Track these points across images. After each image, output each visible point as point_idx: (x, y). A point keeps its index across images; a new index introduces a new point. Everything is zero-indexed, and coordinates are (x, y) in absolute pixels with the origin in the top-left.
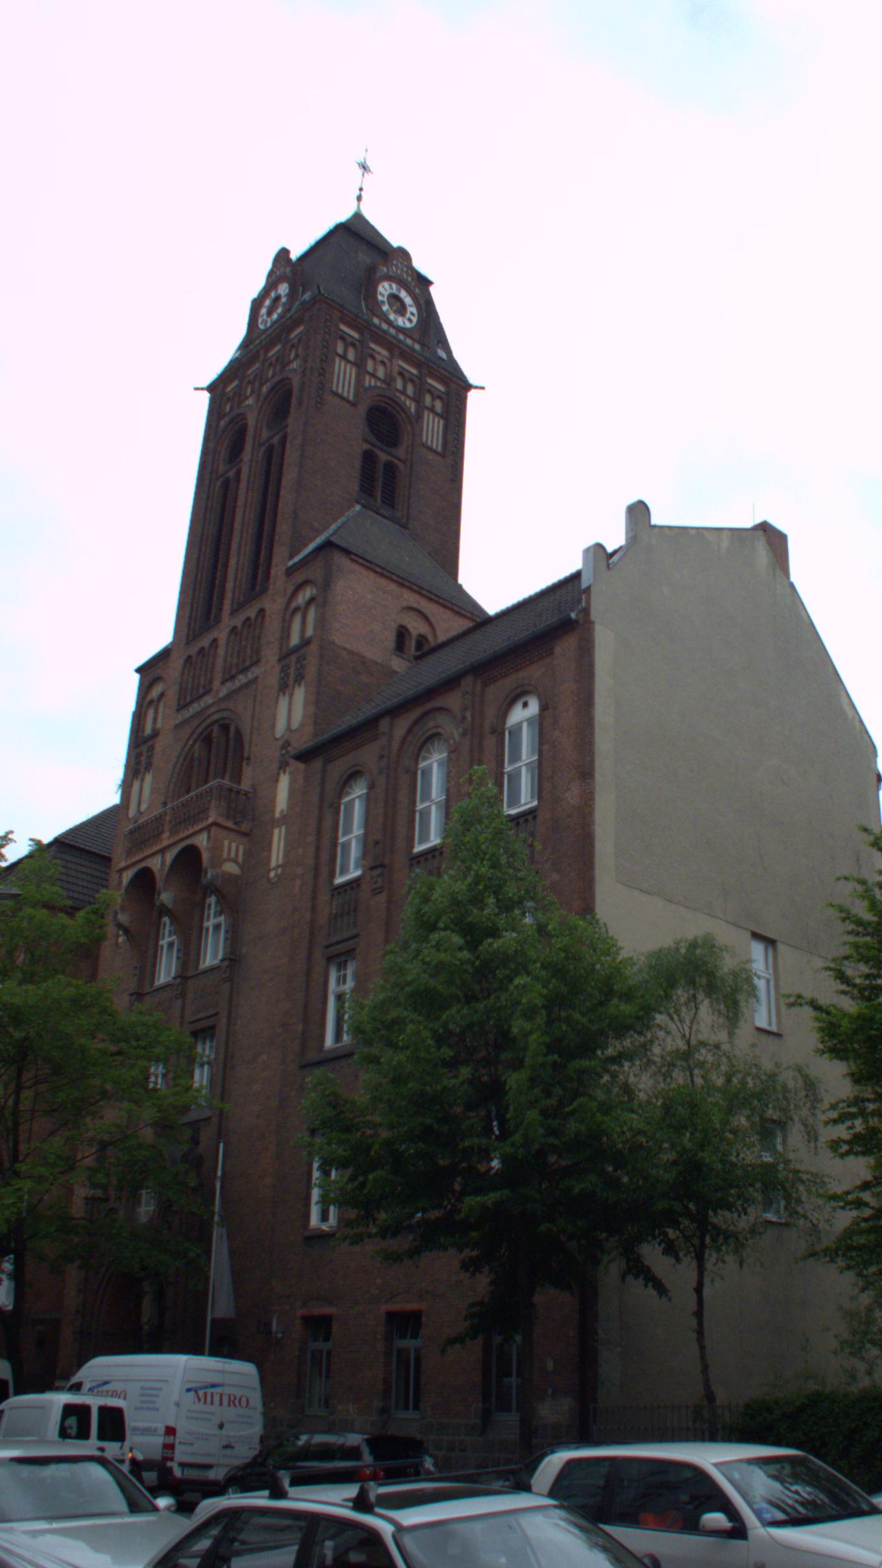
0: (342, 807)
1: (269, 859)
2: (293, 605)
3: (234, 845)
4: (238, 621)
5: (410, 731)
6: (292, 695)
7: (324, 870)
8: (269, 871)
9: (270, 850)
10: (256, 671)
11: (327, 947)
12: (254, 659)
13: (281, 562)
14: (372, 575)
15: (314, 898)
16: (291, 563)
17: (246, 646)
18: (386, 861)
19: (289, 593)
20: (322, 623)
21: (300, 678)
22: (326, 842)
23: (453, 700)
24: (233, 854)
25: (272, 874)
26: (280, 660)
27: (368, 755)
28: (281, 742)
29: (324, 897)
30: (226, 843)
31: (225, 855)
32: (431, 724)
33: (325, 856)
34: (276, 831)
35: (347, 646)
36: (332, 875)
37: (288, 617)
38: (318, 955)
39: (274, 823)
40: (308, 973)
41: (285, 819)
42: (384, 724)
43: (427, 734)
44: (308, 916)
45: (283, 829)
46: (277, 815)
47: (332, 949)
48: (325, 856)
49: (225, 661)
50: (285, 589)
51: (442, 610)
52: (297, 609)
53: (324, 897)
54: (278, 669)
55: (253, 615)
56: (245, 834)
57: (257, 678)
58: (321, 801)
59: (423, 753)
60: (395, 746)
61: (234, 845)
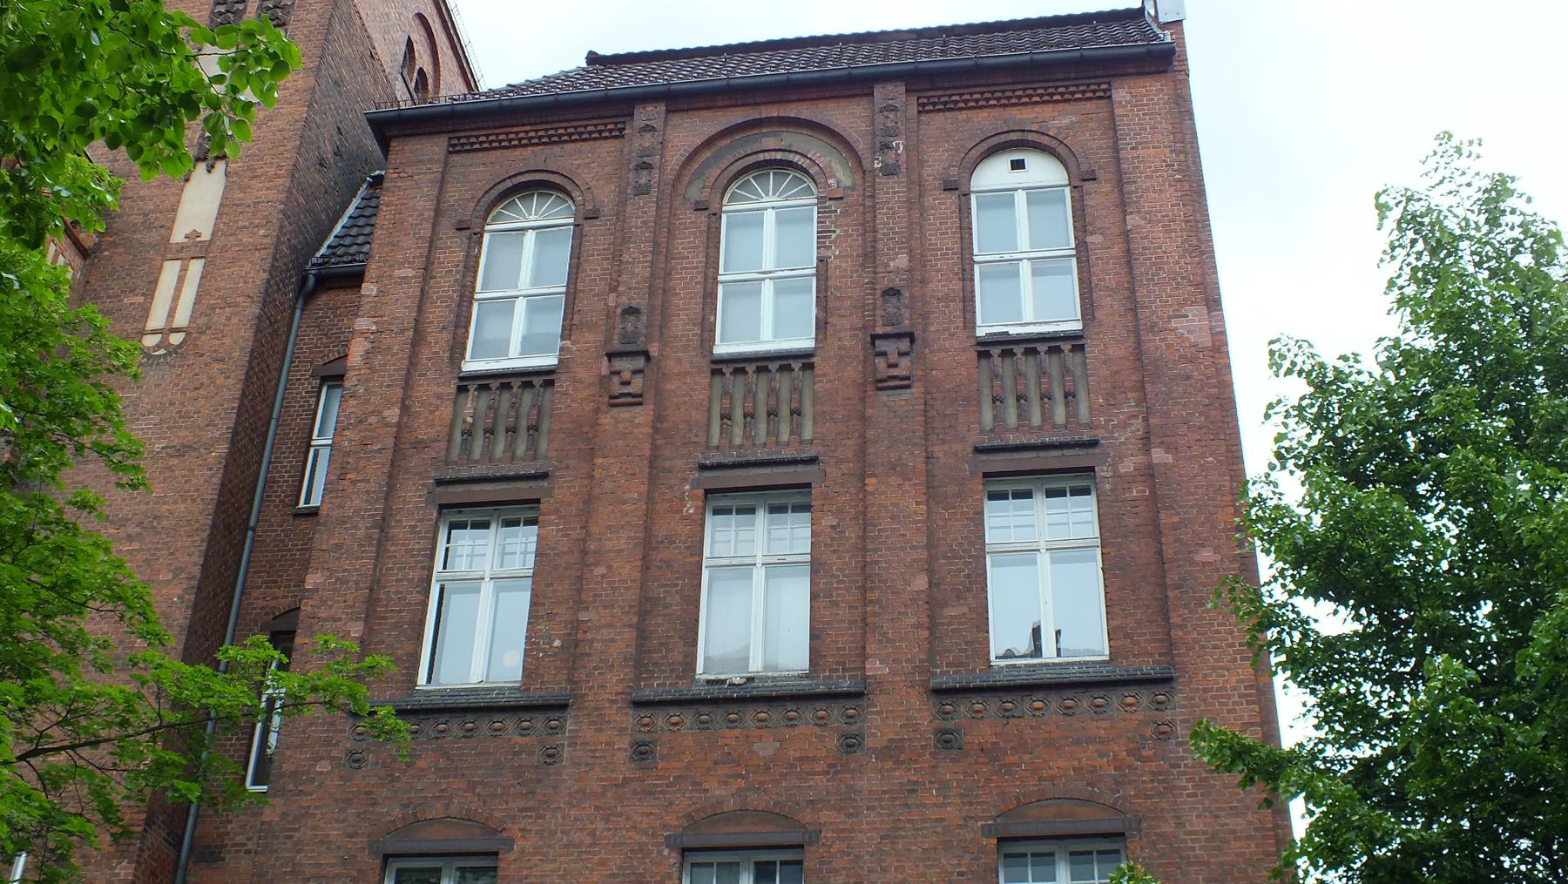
0: (486, 237)
1: (146, 310)
5: (709, 143)
7: (437, 342)
8: (142, 333)
9: (150, 295)
11: (440, 483)
15: (407, 385)
18: (654, 350)
22: (444, 285)
23: (846, 116)
25: (150, 341)
27: (590, 162)
29: (433, 388)
32: (769, 143)
33: (438, 313)
34: (170, 270)
36: (457, 350)
38: (414, 495)
39: (167, 251)
40: (383, 525)
41: (195, 248)
42: (648, 114)
43: (761, 157)
44: (393, 414)
45: (196, 267)
46: (178, 237)
47: (451, 489)
48: (438, 313)
51: (450, 52)
53: (433, 388)
56: (84, 252)
58: (438, 212)
59: (733, 188)
60: (675, 158)
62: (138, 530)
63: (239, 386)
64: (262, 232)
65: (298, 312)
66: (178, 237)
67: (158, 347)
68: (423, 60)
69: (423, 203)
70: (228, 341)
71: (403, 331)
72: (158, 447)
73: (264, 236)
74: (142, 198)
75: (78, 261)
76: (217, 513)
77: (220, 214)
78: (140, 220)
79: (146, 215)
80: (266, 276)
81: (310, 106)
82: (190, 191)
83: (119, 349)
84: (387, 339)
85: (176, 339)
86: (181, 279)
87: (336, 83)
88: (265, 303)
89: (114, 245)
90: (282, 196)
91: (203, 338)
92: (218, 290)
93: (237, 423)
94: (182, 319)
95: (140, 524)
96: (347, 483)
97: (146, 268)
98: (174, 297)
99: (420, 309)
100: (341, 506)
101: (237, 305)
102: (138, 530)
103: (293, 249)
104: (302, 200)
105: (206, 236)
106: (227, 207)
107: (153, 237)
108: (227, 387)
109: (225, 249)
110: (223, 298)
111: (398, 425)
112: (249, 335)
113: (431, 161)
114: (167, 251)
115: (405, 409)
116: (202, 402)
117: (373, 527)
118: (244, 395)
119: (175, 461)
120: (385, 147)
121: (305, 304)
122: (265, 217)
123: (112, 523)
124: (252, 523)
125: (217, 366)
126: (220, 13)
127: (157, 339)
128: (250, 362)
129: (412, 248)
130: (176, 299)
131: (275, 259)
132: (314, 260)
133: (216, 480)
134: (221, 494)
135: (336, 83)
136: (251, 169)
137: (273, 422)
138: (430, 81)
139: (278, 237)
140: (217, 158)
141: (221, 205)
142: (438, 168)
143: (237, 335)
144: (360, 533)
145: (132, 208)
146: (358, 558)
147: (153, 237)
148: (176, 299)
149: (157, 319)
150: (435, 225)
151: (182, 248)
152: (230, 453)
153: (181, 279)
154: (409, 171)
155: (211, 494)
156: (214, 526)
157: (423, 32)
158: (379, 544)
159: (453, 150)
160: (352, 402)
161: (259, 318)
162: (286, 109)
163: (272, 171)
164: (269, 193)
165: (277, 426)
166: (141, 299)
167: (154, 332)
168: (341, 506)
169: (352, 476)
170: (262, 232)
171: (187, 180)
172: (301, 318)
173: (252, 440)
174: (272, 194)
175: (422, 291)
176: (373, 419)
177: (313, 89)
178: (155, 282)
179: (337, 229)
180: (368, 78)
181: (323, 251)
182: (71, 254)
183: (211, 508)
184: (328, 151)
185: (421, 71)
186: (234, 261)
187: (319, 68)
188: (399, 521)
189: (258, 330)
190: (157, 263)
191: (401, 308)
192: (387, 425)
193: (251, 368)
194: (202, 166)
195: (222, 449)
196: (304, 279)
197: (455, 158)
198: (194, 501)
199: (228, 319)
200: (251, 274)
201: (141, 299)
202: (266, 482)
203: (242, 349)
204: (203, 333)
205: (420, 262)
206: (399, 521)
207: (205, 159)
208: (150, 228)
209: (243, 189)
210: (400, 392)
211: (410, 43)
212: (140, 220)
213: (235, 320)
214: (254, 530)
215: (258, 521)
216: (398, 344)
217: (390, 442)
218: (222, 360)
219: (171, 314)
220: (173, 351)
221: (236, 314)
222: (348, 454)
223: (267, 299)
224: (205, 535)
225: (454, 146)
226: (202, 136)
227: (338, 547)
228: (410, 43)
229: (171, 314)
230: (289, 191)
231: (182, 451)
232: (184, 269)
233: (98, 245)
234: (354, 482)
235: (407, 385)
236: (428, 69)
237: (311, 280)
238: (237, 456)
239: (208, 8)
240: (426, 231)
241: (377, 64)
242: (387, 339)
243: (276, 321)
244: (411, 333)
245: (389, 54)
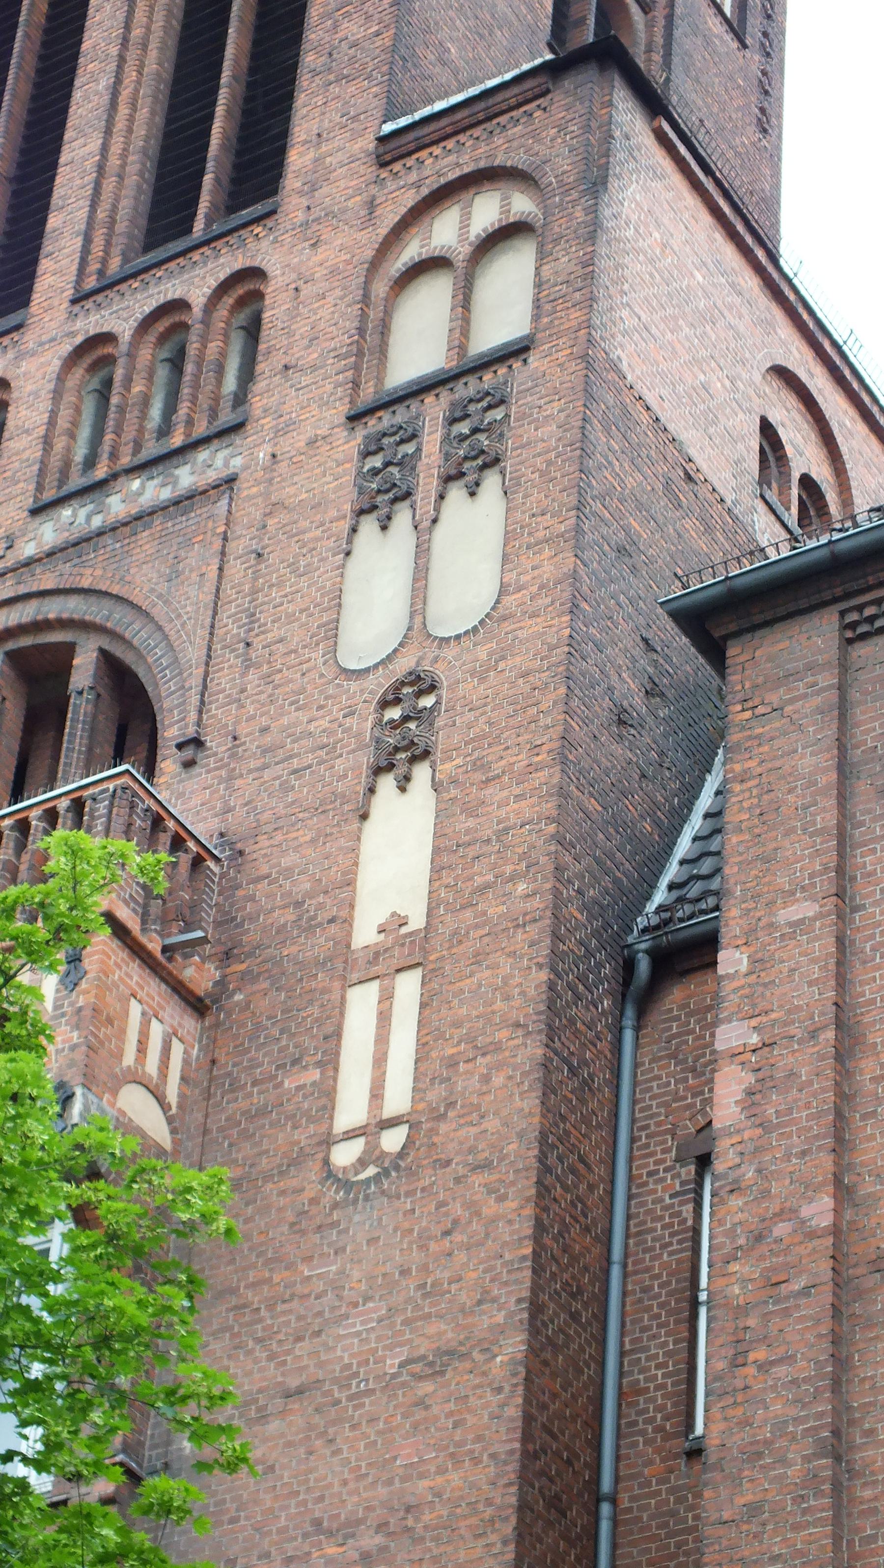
1: (327, 1095)
2: (412, 251)
3: (157, 1030)
4: (121, 315)
6: (425, 530)
8: (328, 1141)
9: (330, 1062)
10: (215, 462)
12: (226, 417)
13: (330, 131)
14: (706, 218)
15: (841, 1141)
16: (388, 128)
17: (145, 401)
19: (390, 217)
20: (574, 296)
21: (469, 467)
24: (152, 1066)
25: (344, 1155)
26: (354, 418)
28: (379, 684)
30: (135, 1010)
31: (129, 1058)
35: (651, 399)
37: (380, 289)
39: (348, 966)
44: (820, 1210)
45: (408, 987)
46: (365, 934)
49: (47, 442)
50: (371, 205)
52: (434, 264)
54: (349, 444)
55: (198, 297)
56: (197, 1005)
57: (231, 480)
58: (845, 770)
61: (157, 1030)
62: (379, 1540)
63: (529, 1211)
64: (522, 887)
65: (628, 1036)
66: (365, 934)
67: (362, 1163)
68: (805, 455)
69: (813, 761)
70: (492, 1124)
71: (813, 1034)
72: (392, 1364)
73: (529, 895)
74: (288, 872)
75: (189, 1024)
76: (524, 1479)
77: (437, 870)
78: (290, 915)
79: (298, 904)
80: (544, 975)
81: (574, 609)
82: (374, 834)
83: (189, 1190)
84: (783, 1059)
85: (393, 1140)
86: (384, 1018)
87: (621, 550)
88: (552, 1033)
89: (248, 977)
90: (549, 807)
91: (443, 1127)
92: (457, 1024)
93: (535, 1289)
94: (398, 1098)
95: (382, 1527)
96: (751, 1370)
97: (315, 1010)
98: (376, 1058)
99: (842, 981)
100: (746, 1422)
101: (497, 1047)
102: (379, 1540)
103: (591, 908)
104: (593, 805)
105: (417, 921)
106: (447, 854)
107: (319, 944)
108: (503, 1221)
109: (457, 938)
110: (470, 1039)
111: (836, 1230)
112: (531, 1103)
113: (810, 668)
114: (348, 966)
115: (843, 1191)
116: (461, 1257)
117: (817, 1456)
118: (540, 1227)
119: (427, 1387)
120: (715, 653)
121: (641, 1014)
122: (523, 856)
123: (330, 1534)
124: (606, 1484)
125: (477, 1180)
126: (375, 472)
127: (357, 1147)
128: (542, 1159)
129: (805, 856)
130: (380, 1060)
131: (556, 937)
132: (641, 922)
133: (514, 1411)
134: (527, 1437)
135: (621, 550)
136: (479, 765)
137: (616, 1272)
138: (831, 497)
139: (556, 893)
140: (413, 760)
141: (437, 851)
142: (828, 679)
143: (508, 1109)
144: (794, 1472)
145: (270, 896)
146: (796, 1527)
147: (319, 944)
148: (380, 1060)
149: (351, 1109)
150: (843, 799)
151: (376, 954)
152: (533, 1351)
153: (384, 1018)
154: (774, 698)
155: (505, 1441)
156: (523, 1507)
157: (792, 401)
158: (837, 1487)
159: (853, 635)
160: (736, 1202)
161: (545, 1065)
162: (535, 626)
163: (521, 760)
164: (522, 806)
165: (625, 1275)
166: (315, 1075)
167: (350, 1135)
168: (746, 1422)
169: (760, 1354)
170: (522, 887)
171: (364, 817)
172: (637, 1046)
173: (575, 1316)
174: (527, 808)
175: (841, 942)
176: (781, 1229)
177: (574, 575)
178: (338, 1034)
179: (684, 846)
180: (690, 525)
181: (660, 896)
182: (175, 1013)
183: (513, 1468)
184: (630, 690)
185: (806, 482)
186: (478, 958)
187: (578, 530)
188: (871, 1432)
189: (548, 1089)
190: (336, 996)
191: (806, 989)
192: (812, 1235)
193: (545, 1168)
194: (387, 784)
195: (514, 1345)
196: (629, 966)
197: (862, 651)
198: (476, 1461)
199: (486, 1079)
200: (515, 979)
201: (315, 1075)
202: (621, 1395)
203: (520, 1135)
204: (442, 1117)
205: (825, 884)
206: (871, 1432)
207: (391, 767)
208: (310, 929)
209: (470, 811)
210: (827, 1161)
211: (767, 429)
212: (290, 915)
213: (498, 1080)
214: (614, 1501)
215: (617, 1479)
216: (807, 1062)
217: (824, 1268)
218: (485, 1166)
219: (377, 1094)
220: (392, 1166)
221: (499, 1066)
222: (742, 1311)
223: (556, 1021)
224: (508, 1528)
225: (853, 626)
226: (379, 723)
227: (754, 1509)
228: (767, 429)
229: (377, 1094)
230: (562, 793)
231: (437, 1364)
232: (387, 997)
233: (221, 984)
234: (764, 1367)
235: (841, 1141)
236: (822, 474)
237: (643, 966)
238: (547, 1355)
239: (351, 468)
240: (826, 816)
241: (703, 491)
242: (783, 1059)
243: (585, 1063)
244: (830, 1034)
245: (726, 462)
